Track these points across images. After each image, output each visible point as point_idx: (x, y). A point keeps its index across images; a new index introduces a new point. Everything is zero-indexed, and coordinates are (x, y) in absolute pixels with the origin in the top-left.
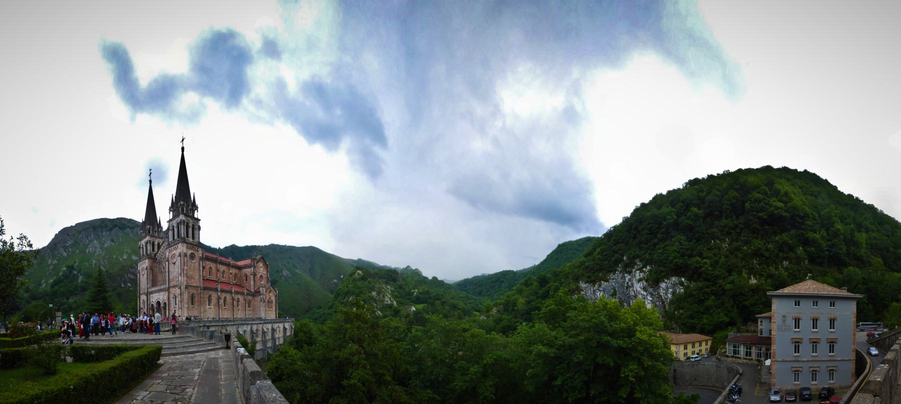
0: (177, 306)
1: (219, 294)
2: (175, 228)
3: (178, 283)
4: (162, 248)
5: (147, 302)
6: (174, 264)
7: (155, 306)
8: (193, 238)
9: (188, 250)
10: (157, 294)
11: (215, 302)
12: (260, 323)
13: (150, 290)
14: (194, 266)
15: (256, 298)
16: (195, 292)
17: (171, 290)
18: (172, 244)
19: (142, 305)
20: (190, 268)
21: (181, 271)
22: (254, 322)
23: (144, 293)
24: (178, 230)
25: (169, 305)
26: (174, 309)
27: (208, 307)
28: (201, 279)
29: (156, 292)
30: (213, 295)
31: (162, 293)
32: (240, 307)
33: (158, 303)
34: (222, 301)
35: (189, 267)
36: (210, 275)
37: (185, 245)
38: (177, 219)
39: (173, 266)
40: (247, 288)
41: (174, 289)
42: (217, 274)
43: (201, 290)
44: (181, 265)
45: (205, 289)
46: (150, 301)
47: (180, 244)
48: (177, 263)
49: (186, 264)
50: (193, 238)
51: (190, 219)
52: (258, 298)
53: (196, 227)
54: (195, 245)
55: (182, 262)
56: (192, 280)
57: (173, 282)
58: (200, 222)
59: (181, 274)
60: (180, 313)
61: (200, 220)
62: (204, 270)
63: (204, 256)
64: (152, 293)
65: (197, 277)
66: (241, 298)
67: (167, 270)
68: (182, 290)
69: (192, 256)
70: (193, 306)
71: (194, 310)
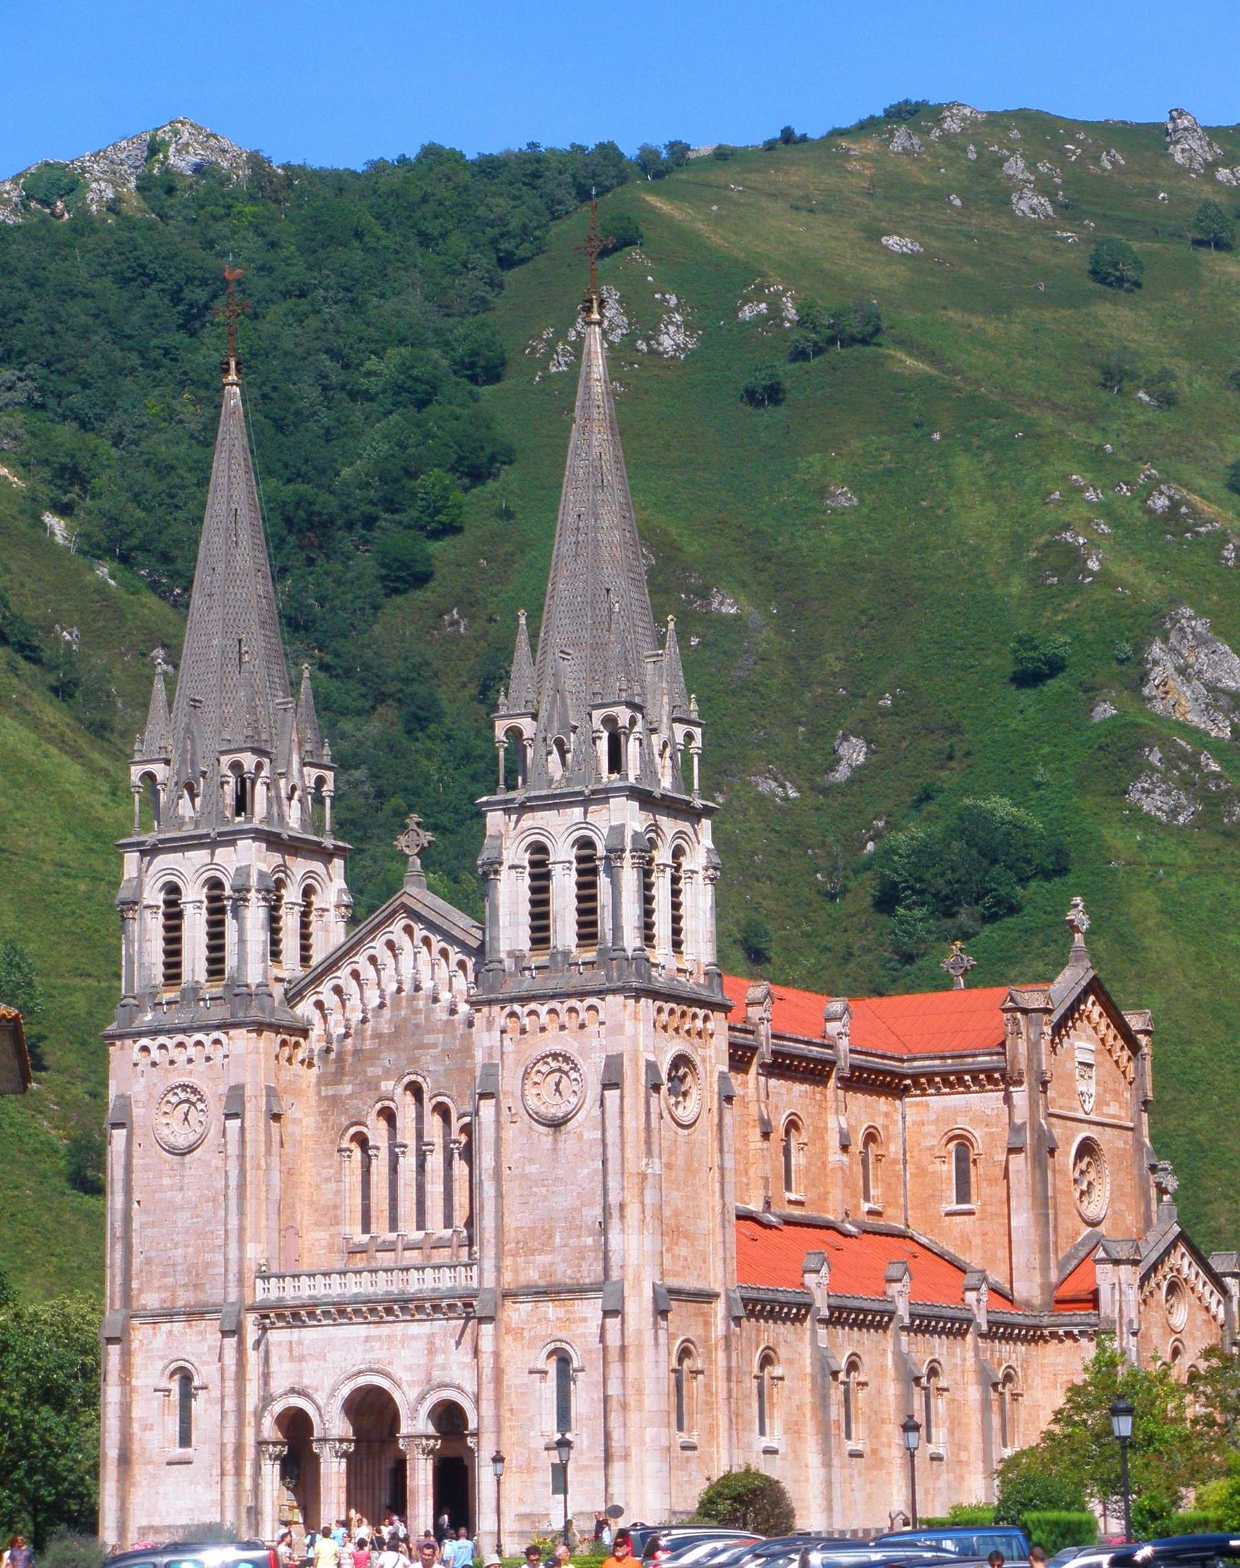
10: (361, 1331)
11: (795, 1400)
25: (499, 1432)
29: (341, 1312)
30: (783, 1352)
31: (415, 1329)
41: (550, 1310)
46: (266, 1377)
48: (584, 1125)
49: (655, 1134)
50: (677, 945)
59: (622, 1207)
68: (631, 1323)
71: (693, 1466)
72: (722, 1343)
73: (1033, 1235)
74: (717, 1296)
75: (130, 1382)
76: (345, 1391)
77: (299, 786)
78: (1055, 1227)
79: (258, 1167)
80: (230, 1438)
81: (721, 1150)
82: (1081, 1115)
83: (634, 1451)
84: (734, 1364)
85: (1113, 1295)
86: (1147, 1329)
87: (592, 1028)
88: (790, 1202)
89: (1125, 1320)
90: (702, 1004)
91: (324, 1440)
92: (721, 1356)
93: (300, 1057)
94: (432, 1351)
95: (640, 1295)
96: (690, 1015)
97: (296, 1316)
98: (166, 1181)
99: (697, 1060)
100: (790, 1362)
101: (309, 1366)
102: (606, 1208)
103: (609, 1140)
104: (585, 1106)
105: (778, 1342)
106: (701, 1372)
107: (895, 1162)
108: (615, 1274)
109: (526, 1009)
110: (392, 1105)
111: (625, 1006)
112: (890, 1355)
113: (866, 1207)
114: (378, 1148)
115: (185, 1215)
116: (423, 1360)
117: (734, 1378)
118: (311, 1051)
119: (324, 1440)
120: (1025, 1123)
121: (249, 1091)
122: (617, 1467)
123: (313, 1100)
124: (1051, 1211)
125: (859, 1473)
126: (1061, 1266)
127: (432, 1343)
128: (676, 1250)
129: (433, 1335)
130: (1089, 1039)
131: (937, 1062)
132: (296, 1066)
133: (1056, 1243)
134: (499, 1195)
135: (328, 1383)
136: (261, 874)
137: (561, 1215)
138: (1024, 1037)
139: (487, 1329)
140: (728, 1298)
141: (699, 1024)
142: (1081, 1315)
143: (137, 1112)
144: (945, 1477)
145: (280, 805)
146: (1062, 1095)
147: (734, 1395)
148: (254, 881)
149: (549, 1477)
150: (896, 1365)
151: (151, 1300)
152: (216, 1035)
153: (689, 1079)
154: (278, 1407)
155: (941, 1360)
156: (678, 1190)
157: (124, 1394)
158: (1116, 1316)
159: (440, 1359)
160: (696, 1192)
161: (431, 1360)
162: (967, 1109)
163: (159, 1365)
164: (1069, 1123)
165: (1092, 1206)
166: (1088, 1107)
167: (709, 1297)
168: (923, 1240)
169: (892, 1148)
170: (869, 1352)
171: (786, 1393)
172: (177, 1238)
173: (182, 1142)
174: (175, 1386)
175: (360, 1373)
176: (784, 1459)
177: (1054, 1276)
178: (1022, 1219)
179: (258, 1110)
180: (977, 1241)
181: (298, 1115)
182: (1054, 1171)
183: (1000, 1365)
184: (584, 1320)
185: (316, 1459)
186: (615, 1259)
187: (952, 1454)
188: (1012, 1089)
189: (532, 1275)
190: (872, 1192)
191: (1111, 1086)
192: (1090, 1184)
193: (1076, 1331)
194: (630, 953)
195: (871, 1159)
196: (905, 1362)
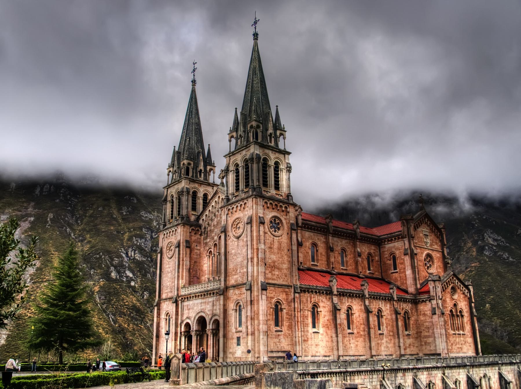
0: (243, 328)
1: (335, 299)
2: (240, 169)
3: (245, 278)
4: (213, 204)
5: (177, 319)
6: (238, 238)
7: (194, 327)
8: (277, 187)
9: (267, 211)
10: (199, 301)
11: (327, 318)
12: (437, 368)
13: (183, 292)
14: (280, 243)
15: (421, 307)
16: (282, 297)
17: (231, 292)
18: (234, 200)
19: (163, 324)
20: (270, 248)
21: (252, 253)
22: (420, 366)
23: (170, 298)
24: (247, 172)
26: (236, 335)
27: (311, 330)
28: (295, 269)
29: (196, 296)
30: (321, 304)
31: (211, 299)
32: (385, 330)
33: (202, 321)
34: (342, 316)
35: (268, 245)
36: (313, 260)
37: (261, 202)
38: (244, 152)
39: (236, 243)
40: (399, 284)
41: (237, 292)
42: (328, 258)
43: (295, 292)
44: (252, 240)
45: (304, 290)
46: (182, 315)
47: (250, 200)
49: (262, 238)
51: (270, 153)
52: (426, 308)
53: (282, 166)
54: (279, 201)
55: (255, 234)
56: (276, 272)
57: (235, 277)
58: (290, 156)
59: (252, 258)
60: (250, 344)
61: (289, 153)
62: (302, 250)
63: (300, 222)
64: (188, 297)
65: (285, 266)
66: (386, 309)
67: (223, 250)
69: (276, 224)
70: (278, 328)
71: (282, 337)
72: (293, 300)
73: (411, 276)
74: (291, 286)
75: (159, 317)
76: (197, 318)
77: (203, 169)
78: (418, 274)
79: (183, 260)
80: (174, 331)
81: (292, 244)
82: (425, 247)
83: (256, 332)
84: (296, 306)
85: (433, 289)
86: (445, 299)
87: (246, 209)
88: (342, 269)
89: (438, 296)
90: (284, 203)
91: (192, 331)
92: (293, 304)
93: (199, 233)
94: (213, 306)
95: (258, 284)
96: (279, 205)
97: (188, 298)
98: (167, 266)
99: (283, 219)
100: (324, 307)
101: (191, 311)
102: (248, 259)
103: (248, 239)
104: (245, 231)
105: (319, 302)
106: (285, 309)
107: (377, 261)
108: (250, 279)
109: (232, 207)
110: (216, 242)
111: (253, 201)
112: (363, 306)
113: (369, 272)
114: (214, 254)
115: (170, 274)
116: (212, 308)
117: (296, 310)
118: (202, 232)
119: (192, 331)
120: (408, 248)
121: (182, 241)
122: (250, 337)
123: (202, 245)
124: (416, 270)
125: (353, 339)
126: (421, 284)
127: (213, 303)
128: (274, 273)
129: (213, 301)
130: (427, 229)
131: (386, 236)
132: (199, 236)
133: (419, 278)
134: (226, 259)
135: (194, 315)
136: (186, 188)
137: (239, 264)
138: (406, 226)
139: (222, 297)
140: (294, 287)
141: (284, 209)
142: (426, 296)
143: (163, 249)
144: (385, 339)
145: (197, 173)
146: (420, 242)
147: (296, 315)
148: (185, 190)
149: (235, 341)
150: (365, 309)
151: (164, 296)
152: (176, 228)
153: (280, 224)
154: (185, 323)
155: (382, 308)
156: (274, 255)
157: (157, 320)
158: (435, 295)
159: (215, 308)
160: (282, 256)
161: (213, 308)
162: (394, 247)
163: (165, 312)
164: (422, 249)
165: (431, 270)
166: (428, 246)
167: (288, 286)
168: (386, 280)
169: (377, 258)
170: (355, 305)
171: (323, 316)
172: (169, 280)
173: (170, 256)
174: (168, 318)
175: (199, 312)
176: (322, 335)
177: (419, 286)
178: (409, 272)
179: (183, 246)
180: (399, 279)
181: (198, 248)
182: (417, 260)
183: (403, 309)
184: (244, 293)
185: (192, 336)
186: (250, 274)
187: (387, 333)
188: (404, 239)
189: (232, 281)
190: (371, 269)
191: (434, 241)
192: (430, 265)
193: (425, 300)
194: (255, 186)
195: (370, 260)
196: (367, 308)
